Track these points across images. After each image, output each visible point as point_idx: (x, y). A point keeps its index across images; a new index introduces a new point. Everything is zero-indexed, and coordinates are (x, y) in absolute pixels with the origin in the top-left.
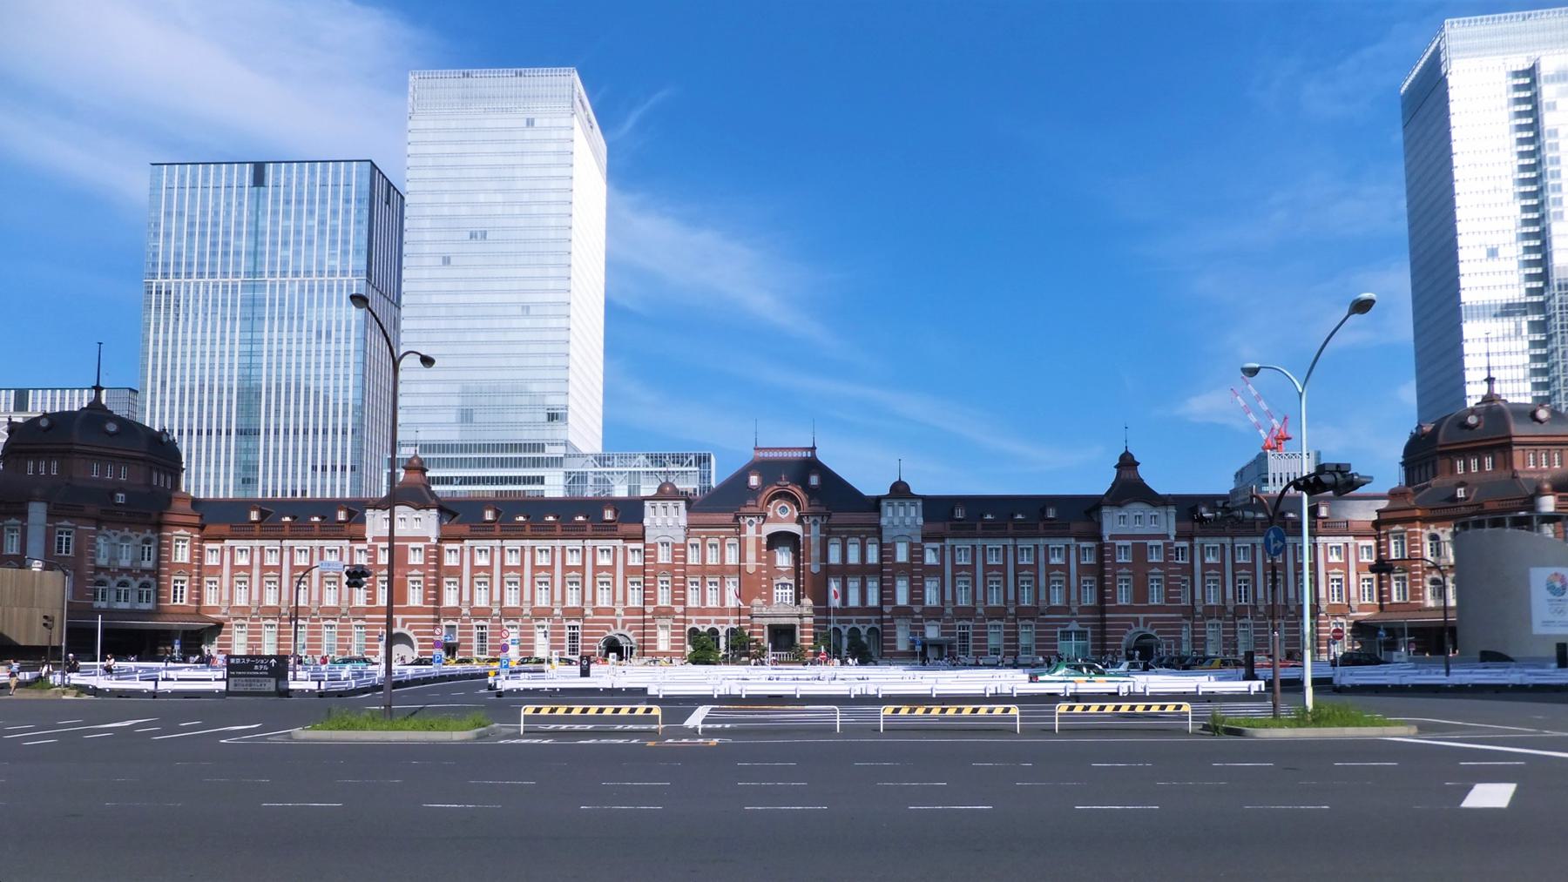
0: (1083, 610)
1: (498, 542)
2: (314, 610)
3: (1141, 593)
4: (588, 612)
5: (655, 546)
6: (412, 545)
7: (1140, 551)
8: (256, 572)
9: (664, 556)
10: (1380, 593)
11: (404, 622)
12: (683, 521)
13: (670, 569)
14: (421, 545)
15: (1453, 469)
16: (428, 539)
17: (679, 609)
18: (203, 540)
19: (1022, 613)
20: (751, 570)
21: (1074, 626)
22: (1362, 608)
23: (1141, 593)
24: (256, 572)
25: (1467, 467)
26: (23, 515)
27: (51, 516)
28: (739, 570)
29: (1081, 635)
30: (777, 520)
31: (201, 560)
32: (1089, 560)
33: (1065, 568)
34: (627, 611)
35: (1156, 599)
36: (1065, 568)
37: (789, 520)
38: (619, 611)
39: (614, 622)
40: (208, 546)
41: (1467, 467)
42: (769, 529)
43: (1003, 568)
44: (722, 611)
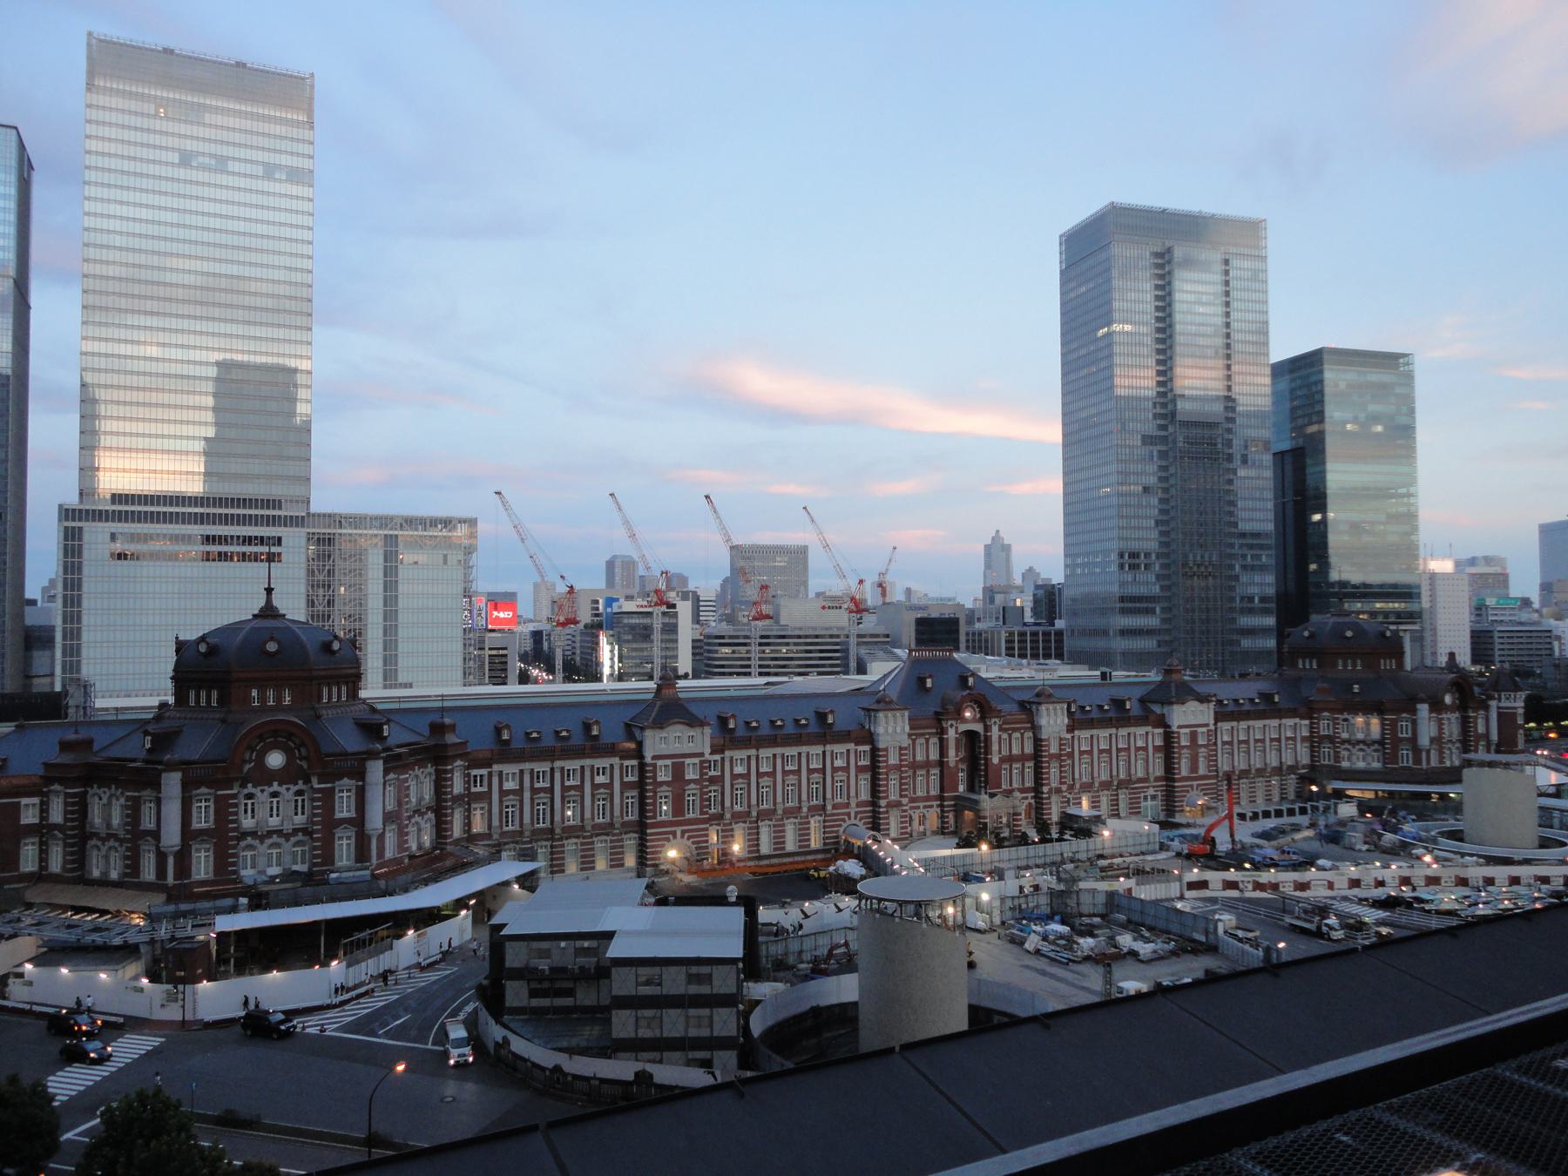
0: (1157, 779)
1: (753, 752)
2: (589, 828)
3: (1194, 767)
4: (829, 807)
5: (886, 750)
6: (688, 761)
7: (1193, 736)
8: (527, 795)
9: (893, 760)
10: (1312, 756)
11: (683, 832)
12: (907, 728)
13: (898, 768)
14: (696, 760)
15: (1336, 665)
16: (702, 755)
17: (905, 801)
18: (468, 768)
19: (1122, 784)
20: (952, 764)
21: (1151, 791)
22: (1304, 767)
23: (1194, 767)
24: (527, 795)
25: (1345, 665)
26: (360, 774)
27: (386, 772)
28: (941, 764)
29: (1154, 797)
30: (964, 720)
31: (468, 789)
32: (1159, 742)
33: (1145, 749)
34: (858, 805)
35: (1202, 771)
36: (1145, 749)
37: (974, 720)
38: (853, 804)
39: (849, 814)
40: (474, 772)
41: (1345, 665)
42: (963, 727)
43: (1109, 751)
44: (928, 798)
